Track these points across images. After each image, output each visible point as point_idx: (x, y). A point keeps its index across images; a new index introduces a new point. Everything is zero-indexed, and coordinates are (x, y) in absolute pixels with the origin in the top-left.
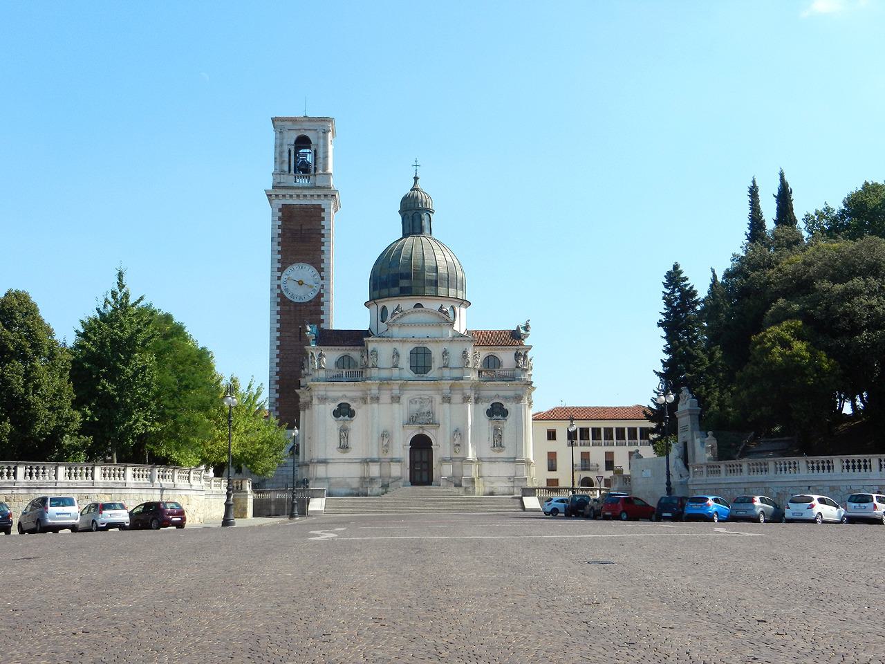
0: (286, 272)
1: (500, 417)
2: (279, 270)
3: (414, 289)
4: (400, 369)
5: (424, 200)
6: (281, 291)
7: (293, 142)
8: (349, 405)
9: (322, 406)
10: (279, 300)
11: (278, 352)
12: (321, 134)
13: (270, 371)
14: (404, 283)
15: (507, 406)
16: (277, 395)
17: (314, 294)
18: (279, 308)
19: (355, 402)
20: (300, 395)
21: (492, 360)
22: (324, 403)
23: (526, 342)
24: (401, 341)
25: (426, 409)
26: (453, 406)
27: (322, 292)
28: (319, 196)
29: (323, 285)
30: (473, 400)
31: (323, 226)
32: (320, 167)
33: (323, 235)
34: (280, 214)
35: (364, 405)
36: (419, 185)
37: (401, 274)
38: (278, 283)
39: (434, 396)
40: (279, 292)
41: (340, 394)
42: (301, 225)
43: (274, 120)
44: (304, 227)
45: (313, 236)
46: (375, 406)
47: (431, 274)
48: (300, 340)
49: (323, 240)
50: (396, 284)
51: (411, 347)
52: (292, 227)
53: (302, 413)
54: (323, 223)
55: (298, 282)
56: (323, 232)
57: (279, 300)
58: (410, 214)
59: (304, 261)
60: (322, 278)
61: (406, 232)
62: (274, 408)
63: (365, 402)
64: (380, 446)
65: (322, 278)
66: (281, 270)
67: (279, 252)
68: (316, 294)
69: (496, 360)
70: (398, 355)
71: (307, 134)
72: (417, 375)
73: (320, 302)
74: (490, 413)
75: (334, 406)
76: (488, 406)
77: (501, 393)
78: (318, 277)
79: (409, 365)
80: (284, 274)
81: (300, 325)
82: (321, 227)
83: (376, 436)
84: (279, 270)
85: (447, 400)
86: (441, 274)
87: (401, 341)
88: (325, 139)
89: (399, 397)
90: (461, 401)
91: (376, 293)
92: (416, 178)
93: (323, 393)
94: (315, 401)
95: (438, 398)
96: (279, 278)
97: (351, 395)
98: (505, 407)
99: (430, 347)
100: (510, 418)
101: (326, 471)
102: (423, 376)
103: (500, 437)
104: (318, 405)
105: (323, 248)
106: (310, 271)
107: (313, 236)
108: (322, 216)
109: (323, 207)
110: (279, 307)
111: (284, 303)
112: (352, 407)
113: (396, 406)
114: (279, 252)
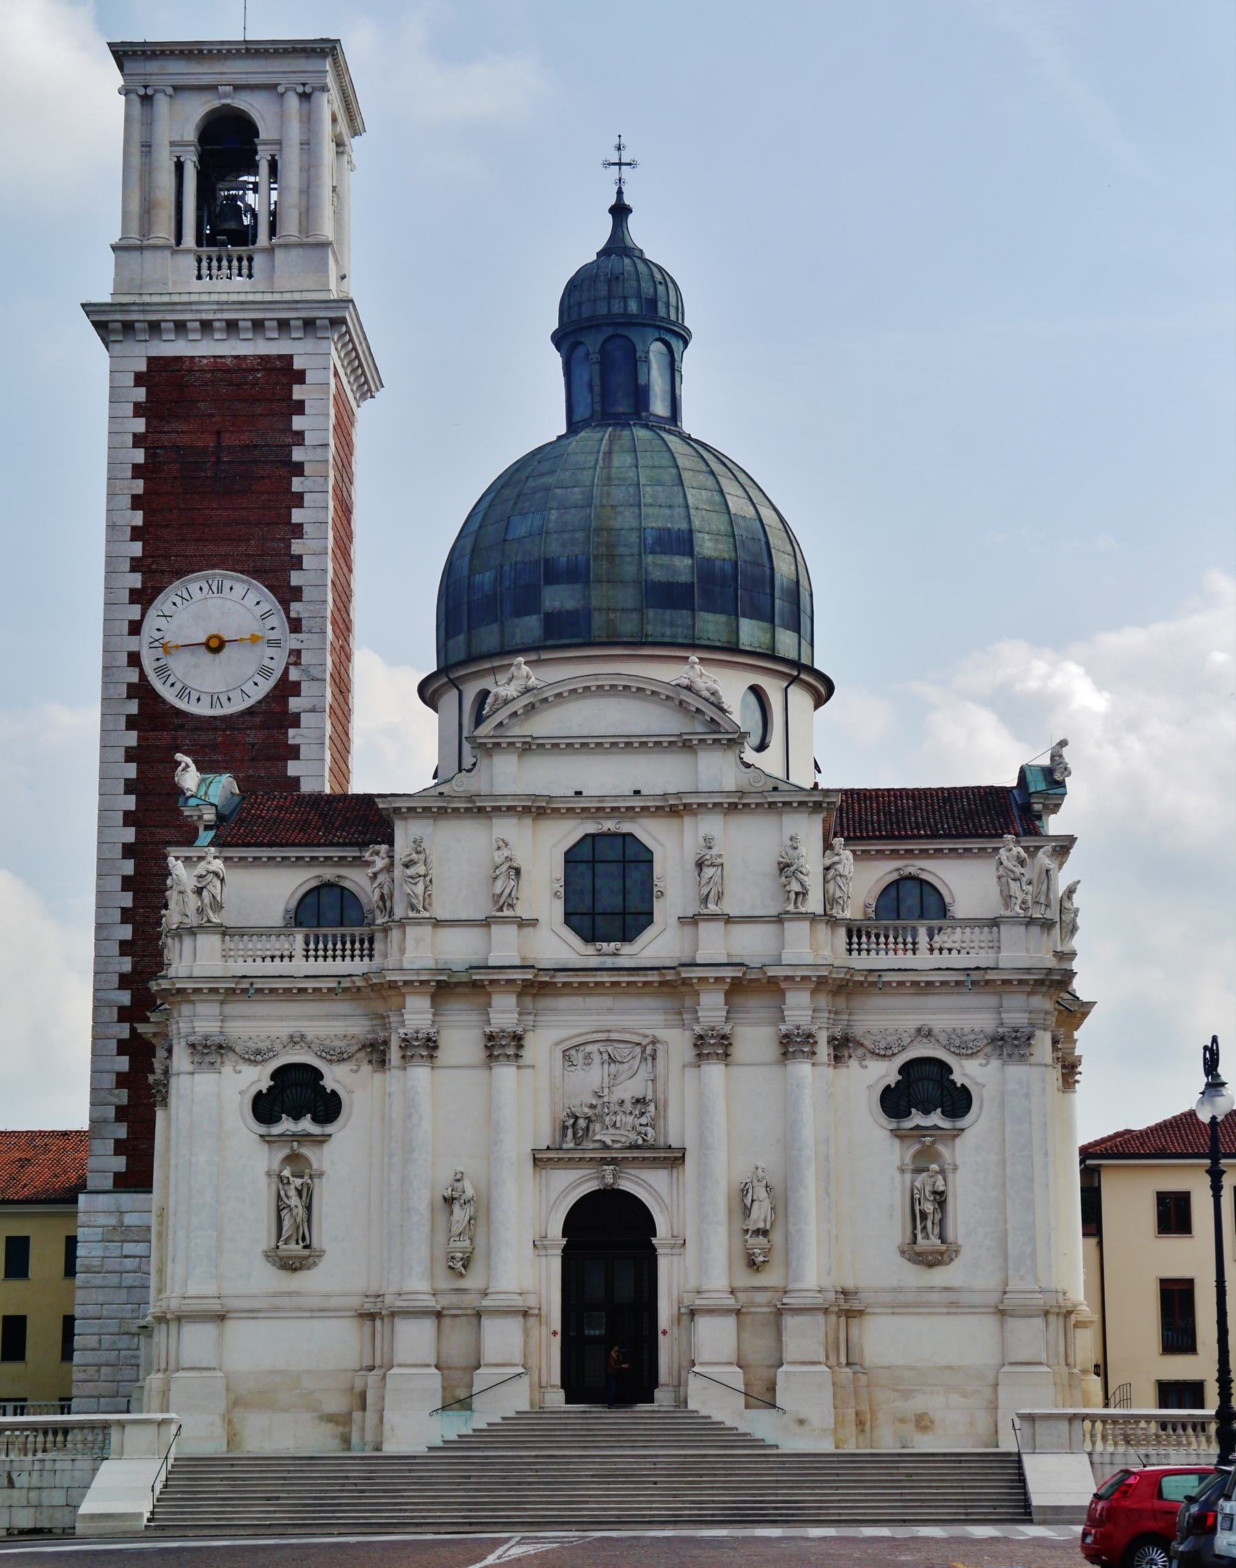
0: (164, 603)
1: (936, 1119)
2: (136, 596)
3: (598, 620)
4: (522, 923)
5: (646, 286)
6: (142, 675)
7: (191, 135)
8: (318, 1075)
10: (133, 707)
11: (127, 900)
12: (293, 102)
13: (96, 973)
14: (559, 598)
15: (965, 1072)
16: (123, 1063)
17: (266, 686)
18: (132, 738)
19: (341, 1058)
20: (154, 1041)
21: (911, 899)
23: (1055, 825)
24: (527, 810)
25: (630, 1088)
26: (734, 1070)
27: (294, 675)
28: (283, 325)
29: (296, 653)
30: (823, 1050)
31: (300, 435)
32: (290, 227)
33: (298, 469)
34: (141, 394)
35: (378, 1076)
36: (638, 231)
37: (549, 564)
38: (132, 644)
39: (661, 1034)
40: (135, 678)
41: (283, 1030)
42: (218, 433)
43: (123, 54)
44: (227, 440)
46: (420, 1074)
47: (664, 559)
50: (527, 602)
51: (569, 832)
53: (160, 1114)
54: (298, 423)
55: (207, 645)
56: (297, 455)
58: (592, 342)
60: (295, 626)
61: (582, 412)
62: (111, 1112)
63: (382, 1062)
64: (441, 1238)
66: (143, 597)
67: (136, 534)
68: (272, 682)
69: (931, 901)
70: (518, 871)
71: (243, 102)
72: (590, 949)
75: (258, 1078)
76: (886, 1073)
78: (278, 620)
79: (559, 906)
80: (152, 612)
82: (289, 440)
83: (422, 1199)
84: (136, 596)
86: (709, 561)
87: (527, 810)
88: (309, 121)
89: (518, 1039)
90: (771, 1050)
92: (620, 211)
94: (181, 1060)
95: (677, 1042)
96: (135, 628)
97: (322, 1033)
98: (958, 1078)
99: (649, 832)
100: (977, 1122)
102: (615, 955)
103: (940, 1199)
104: (193, 1073)
105: (297, 516)
106: (252, 598)
108: (296, 396)
109: (297, 365)
110: (134, 734)
112: (329, 1083)
113: (506, 1074)
114: (136, 534)
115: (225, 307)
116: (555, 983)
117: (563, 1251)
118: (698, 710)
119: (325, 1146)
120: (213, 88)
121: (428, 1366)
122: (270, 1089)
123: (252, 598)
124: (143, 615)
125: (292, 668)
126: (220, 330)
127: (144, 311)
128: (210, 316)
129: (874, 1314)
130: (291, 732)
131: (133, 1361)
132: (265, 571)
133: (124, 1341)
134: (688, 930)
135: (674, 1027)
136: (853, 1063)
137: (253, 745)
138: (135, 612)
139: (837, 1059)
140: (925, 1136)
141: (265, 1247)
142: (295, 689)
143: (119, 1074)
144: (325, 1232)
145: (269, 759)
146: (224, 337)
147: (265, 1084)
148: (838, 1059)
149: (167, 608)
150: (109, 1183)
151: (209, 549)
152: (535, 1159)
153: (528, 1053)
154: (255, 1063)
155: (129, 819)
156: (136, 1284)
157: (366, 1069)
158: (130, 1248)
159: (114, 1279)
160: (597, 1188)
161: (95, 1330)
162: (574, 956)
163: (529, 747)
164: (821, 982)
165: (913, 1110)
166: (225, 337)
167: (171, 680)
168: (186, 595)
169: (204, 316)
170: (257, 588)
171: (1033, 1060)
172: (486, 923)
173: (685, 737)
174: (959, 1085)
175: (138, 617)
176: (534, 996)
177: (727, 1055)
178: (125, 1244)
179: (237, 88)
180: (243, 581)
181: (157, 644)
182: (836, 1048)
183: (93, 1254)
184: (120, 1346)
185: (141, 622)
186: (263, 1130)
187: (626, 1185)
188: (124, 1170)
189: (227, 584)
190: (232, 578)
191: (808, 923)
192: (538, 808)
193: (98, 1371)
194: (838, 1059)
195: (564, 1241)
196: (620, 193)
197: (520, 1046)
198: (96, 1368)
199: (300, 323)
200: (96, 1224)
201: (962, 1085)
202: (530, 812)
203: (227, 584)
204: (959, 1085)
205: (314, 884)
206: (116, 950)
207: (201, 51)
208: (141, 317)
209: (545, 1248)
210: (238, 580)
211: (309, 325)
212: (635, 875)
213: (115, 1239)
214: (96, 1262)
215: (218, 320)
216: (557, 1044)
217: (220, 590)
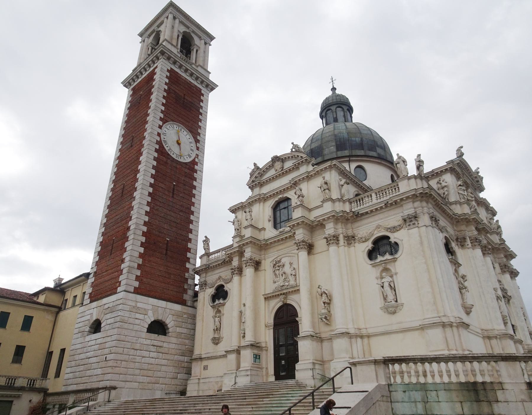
2: (161, 119)
10: (157, 147)
27: (197, 160)
28: (202, 82)
29: (197, 155)
33: (201, 114)
38: (159, 131)
40: (159, 140)
45: (194, 110)
48: (173, 197)
49: (200, 117)
52: (177, 91)
56: (201, 111)
57: (157, 147)
59: (183, 124)
60: (198, 149)
65: (198, 149)
73: (194, 168)
78: (194, 145)
80: (164, 125)
81: (175, 181)
96: (160, 127)
107: (194, 110)
109: (202, 92)
111: (162, 152)
115: (193, 69)
120: (188, 27)
123: (188, 137)
124: (163, 125)
125: (196, 158)
126: (189, 73)
127: (175, 57)
128: (189, 68)
130: (195, 174)
131: (134, 361)
132: (192, 132)
133: (132, 352)
137: (186, 173)
138: (161, 123)
142: (196, 164)
143: (140, 253)
145: (189, 178)
146: (189, 75)
149: (168, 127)
150: (133, 291)
151: (180, 119)
155: (152, 176)
156: (138, 330)
158: (138, 316)
159: (131, 327)
161: (122, 346)
166: (189, 75)
167: (167, 145)
168: (173, 126)
169: (187, 67)
170: (189, 135)
175: (161, 125)
178: (137, 314)
179: (193, 32)
180: (187, 131)
181: (164, 134)
183: (125, 315)
184: (131, 353)
185: (162, 126)
188: (138, 287)
189: (183, 130)
190: (184, 129)
193: (121, 363)
196: (333, 86)
198: (121, 362)
199: (206, 83)
200: (128, 304)
203: (183, 130)
206: (144, 213)
207: (189, 18)
208: (174, 57)
210: (185, 130)
211: (207, 86)
213: (134, 311)
214: (126, 319)
215: (190, 70)
217: (181, 130)
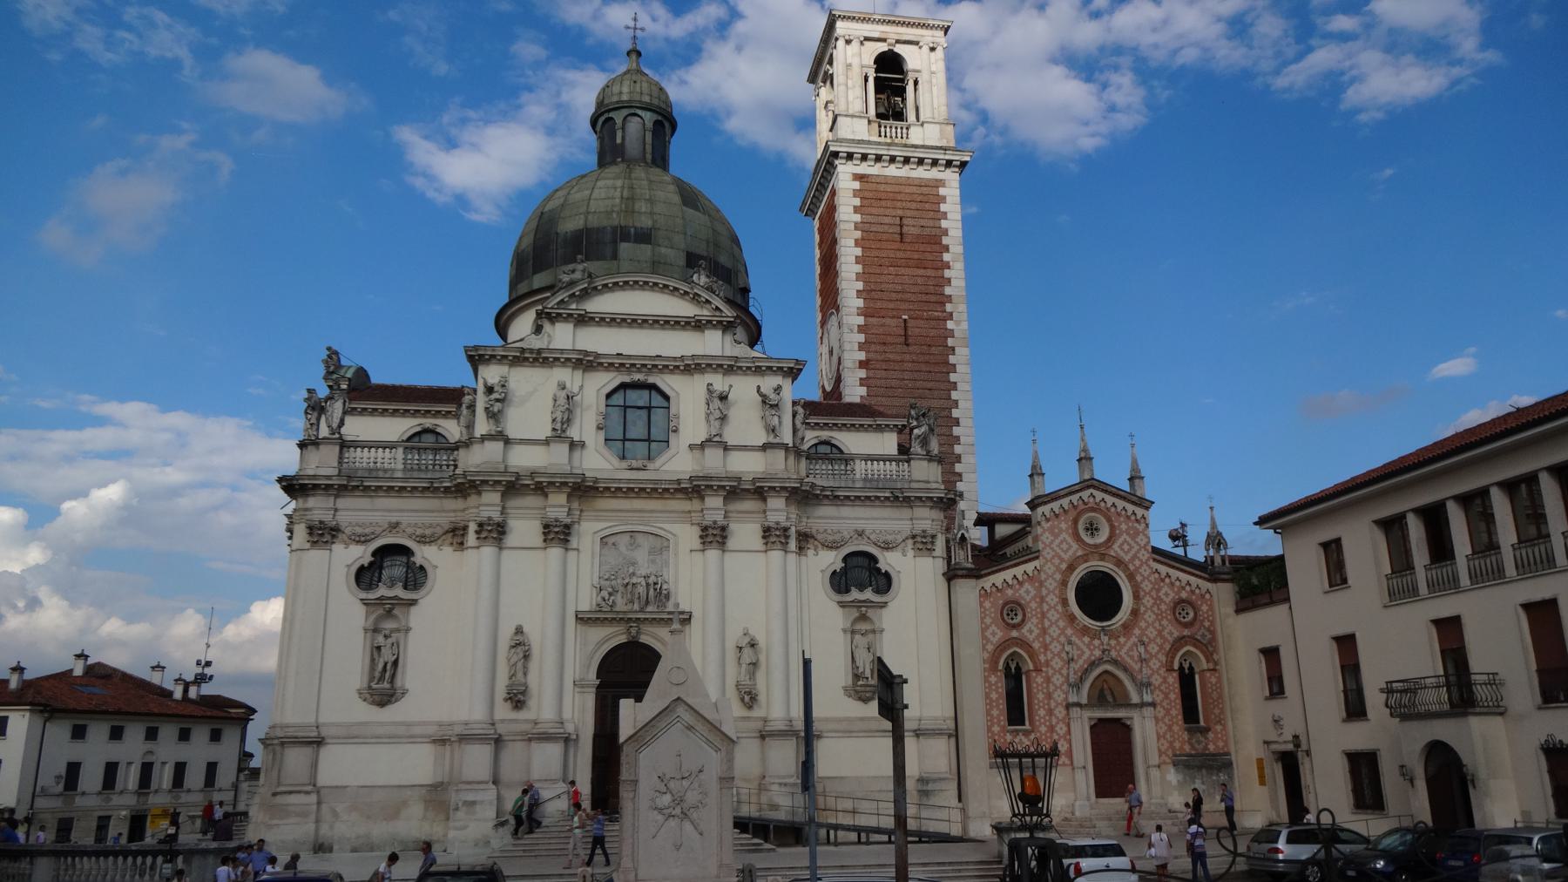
1: (868, 594)
4: (574, 445)
9: (318, 555)
15: (889, 561)
22: (327, 544)
30: (793, 545)
46: (488, 551)
51: (609, 380)
63: (461, 545)
72: (624, 464)
74: (840, 582)
75: (360, 554)
76: (831, 560)
77: (868, 526)
85: (715, 536)
91: (523, 288)
93: (327, 517)
95: (686, 535)
98: (882, 566)
99: (667, 382)
101: (314, 765)
102: (644, 469)
112: (418, 560)
116: (597, 488)
117: (597, 688)
118: (707, 302)
119: (413, 610)
121: (487, 783)
122: (371, 564)
129: (827, 737)
134: (697, 453)
135: (684, 522)
136: (811, 552)
139: (800, 548)
140: (861, 607)
141: (358, 687)
144: (410, 677)
147: (367, 560)
148: (801, 549)
152: (576, 616)
153: (574, 543)
154: (363, 542)
157: (448, 550)
160: (626, 641)
162: (611, 467)
163: (583, 320)
164: (794, 491)
165: (853, 588)
171: (935, 554)
172: (547, 442)
173: (696, 318)
174: (883, 571)
176: (580, 497)
177: (724, 543)
182: (800, 541)
186: (364, 595)
187: (644, 639)
191: (783, 452)
192: (588, 361)
194: (801, 549)
195: (598, 682)
197: (569, 534)
201: (886, 571)
202: (582, 364)
204: (883, 571)
205: (418, 429)
209: (582, 686)
212: (658, 416)
216: (595, 533)
